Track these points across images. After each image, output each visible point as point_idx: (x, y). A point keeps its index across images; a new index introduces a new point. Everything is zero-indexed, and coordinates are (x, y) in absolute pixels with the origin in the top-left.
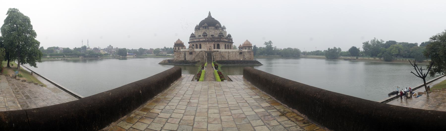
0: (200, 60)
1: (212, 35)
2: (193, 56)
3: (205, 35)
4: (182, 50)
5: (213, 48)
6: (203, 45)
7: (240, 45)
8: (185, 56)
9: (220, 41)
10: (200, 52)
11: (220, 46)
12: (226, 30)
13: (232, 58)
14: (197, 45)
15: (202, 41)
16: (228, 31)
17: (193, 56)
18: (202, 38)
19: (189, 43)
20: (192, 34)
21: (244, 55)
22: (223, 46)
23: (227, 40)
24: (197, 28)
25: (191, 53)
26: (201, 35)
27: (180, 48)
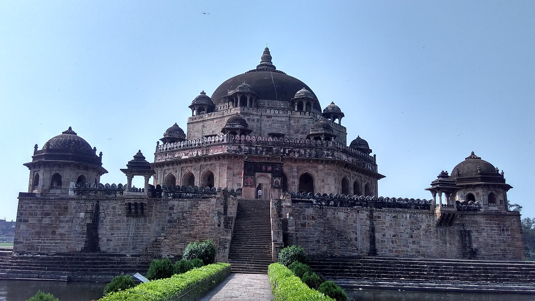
1: (273, 135)
7: (444, 175)
9: (318, 160)
11: (317, 184)
12: (344, 122)
14: (190, 178)
15: (218, 157)
18: (219, 144)
21: (465, 235)
26: (218, 131)
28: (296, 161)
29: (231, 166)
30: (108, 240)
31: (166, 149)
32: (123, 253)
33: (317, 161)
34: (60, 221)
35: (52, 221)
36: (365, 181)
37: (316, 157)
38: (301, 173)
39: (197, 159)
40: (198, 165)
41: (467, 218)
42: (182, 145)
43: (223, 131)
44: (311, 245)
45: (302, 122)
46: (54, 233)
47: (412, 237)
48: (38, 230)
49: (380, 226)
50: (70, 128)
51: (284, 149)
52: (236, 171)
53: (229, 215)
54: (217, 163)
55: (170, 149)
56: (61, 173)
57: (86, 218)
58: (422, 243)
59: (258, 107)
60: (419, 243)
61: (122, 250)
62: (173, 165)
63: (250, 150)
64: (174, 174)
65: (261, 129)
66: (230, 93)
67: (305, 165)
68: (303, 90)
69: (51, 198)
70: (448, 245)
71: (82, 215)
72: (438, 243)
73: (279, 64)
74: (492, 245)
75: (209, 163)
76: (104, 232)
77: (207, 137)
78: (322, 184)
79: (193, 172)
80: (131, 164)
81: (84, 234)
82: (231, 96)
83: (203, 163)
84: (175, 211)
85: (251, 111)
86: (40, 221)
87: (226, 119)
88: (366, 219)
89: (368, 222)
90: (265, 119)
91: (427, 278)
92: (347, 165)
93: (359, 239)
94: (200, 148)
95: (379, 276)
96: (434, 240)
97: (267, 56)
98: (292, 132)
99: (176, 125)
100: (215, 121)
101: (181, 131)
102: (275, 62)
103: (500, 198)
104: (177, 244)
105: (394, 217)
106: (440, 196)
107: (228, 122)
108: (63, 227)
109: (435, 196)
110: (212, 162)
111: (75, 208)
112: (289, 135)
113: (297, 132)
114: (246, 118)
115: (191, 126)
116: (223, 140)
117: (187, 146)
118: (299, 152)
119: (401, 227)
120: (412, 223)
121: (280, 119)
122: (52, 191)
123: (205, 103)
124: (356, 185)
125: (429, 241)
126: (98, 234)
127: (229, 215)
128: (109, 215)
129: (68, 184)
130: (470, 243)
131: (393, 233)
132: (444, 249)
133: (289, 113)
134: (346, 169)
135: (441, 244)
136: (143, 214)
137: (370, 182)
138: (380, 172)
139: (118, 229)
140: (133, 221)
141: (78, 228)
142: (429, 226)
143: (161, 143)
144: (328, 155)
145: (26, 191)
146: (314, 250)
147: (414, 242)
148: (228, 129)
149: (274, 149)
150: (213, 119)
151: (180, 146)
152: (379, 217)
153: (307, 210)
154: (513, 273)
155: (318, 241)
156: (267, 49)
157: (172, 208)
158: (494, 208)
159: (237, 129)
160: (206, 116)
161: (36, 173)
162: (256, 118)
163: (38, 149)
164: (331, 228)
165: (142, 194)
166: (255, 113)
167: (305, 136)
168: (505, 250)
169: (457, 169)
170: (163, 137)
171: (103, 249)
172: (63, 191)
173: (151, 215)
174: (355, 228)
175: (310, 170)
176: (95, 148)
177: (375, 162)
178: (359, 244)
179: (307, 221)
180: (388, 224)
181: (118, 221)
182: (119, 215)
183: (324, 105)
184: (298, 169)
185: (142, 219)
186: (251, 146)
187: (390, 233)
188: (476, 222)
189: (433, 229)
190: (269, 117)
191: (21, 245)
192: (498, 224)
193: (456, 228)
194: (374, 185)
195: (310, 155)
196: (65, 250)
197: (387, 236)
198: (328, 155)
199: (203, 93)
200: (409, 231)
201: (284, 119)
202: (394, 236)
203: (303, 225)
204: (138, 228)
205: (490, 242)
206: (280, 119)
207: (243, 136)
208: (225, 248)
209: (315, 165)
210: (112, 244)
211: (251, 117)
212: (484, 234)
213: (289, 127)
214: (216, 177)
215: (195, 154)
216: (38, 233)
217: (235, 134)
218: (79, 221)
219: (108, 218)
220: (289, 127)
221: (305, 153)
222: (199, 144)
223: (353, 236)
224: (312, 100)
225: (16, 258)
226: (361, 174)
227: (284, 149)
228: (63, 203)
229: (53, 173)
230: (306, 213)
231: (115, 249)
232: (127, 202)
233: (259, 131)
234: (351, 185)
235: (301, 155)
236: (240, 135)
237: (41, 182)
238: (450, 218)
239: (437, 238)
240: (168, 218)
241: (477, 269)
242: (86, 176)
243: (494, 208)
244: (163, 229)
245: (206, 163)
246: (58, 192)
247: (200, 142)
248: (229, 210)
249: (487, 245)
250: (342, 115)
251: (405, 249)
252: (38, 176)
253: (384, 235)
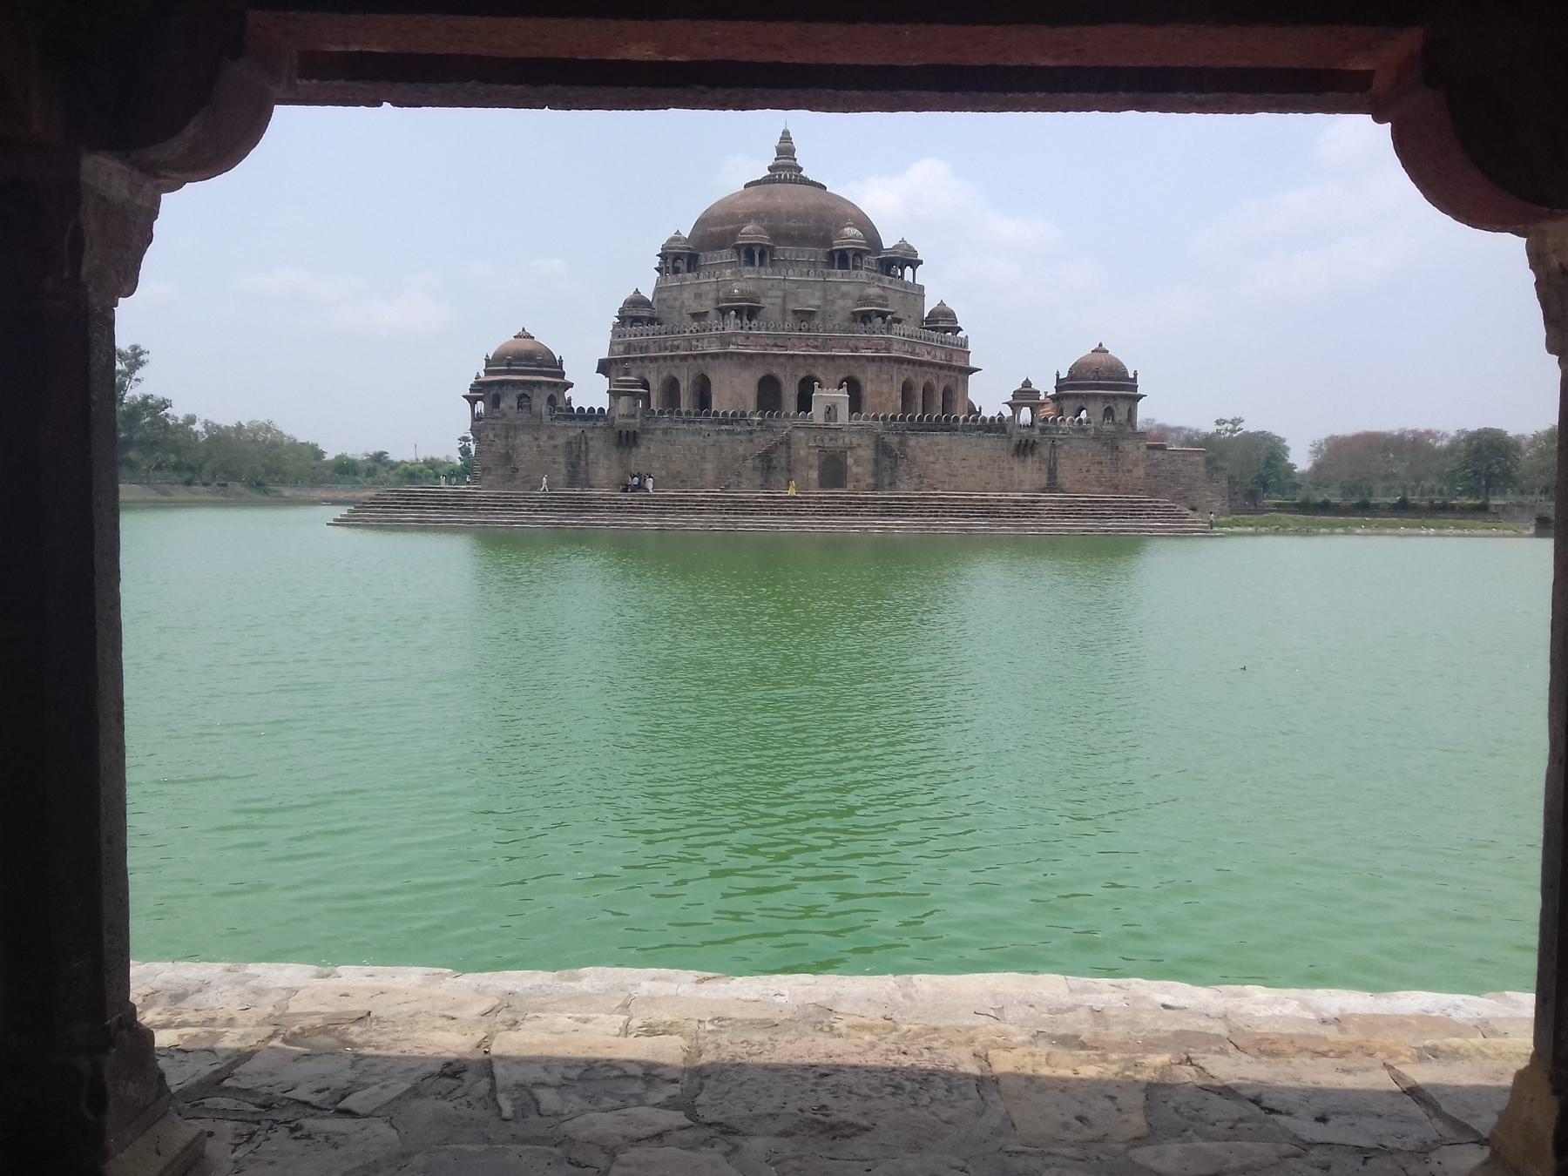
12: (923, 276)
14: (672, 386)
15: (715, 356)
16: (936, 285)
19: (604, 367)
20: (636, 302)
24: (678, 259)
26: (708, 305)
124: (928, 389)
138: (972, 364)
183: (888, 243)
194: (960, 387)
250: (915, 264)
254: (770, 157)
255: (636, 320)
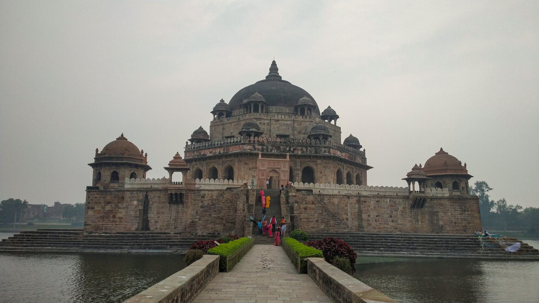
0: (219, 228)
2: (188, 213)
3: (250, 133)
4: (129, 184)
5: (285, 177)
6: (240, 170)
8: (145, 210)
10: (221, 193)
11: (317, 175)
12: (339, 123)
13: (377, 222)
15: (236, 155)
16: (347, 127)
17: (188, 213)
18: (236, 144)
21: (433, 214)
22: (332, 177)
23: (343, 155)
24: (221, 111)
25: (176, 197)
26: (236, 133)
27: (125, 173)
28: (299, 157)
29: (248, 162)
30: (156, 222)
31: (194, 148)
32: (166, 231)
33: (316, 157)
34: (119, 208)
35: (112, 208)
36: (356, 172)
37: (316, 152)
38: (303, 167)
39: (220, 156)
40: (220, 161)
41: (435, 202)
42: (207, 145)
43: (240, 133)
44: (312, 224)
45: (304, 125)
46: (114, 217)
47: (391, 217)
48: (102, 215)
49: (366, 208)
50: (122, 135)
51: (290, 148)
52: (251, 166)
53: (250, 203)
54: (236, 160)
55: (197, 148)
56: (118, 171)
57: (138, 205)
58: (399, 221)
59: (267, 112)
60: (397, 221)
61: (166, 229)
62: (200, 161)
63: (263, 150)
64: (201, 168)
65: (270, 131)
66: (245, 101)
67: (307, 160)
68: (305, 98)
69: (112, 190)
70: (420, 223)
71: (135, 203)
72: (411, 221)
73: (285, 74)
74: (455, 223)
75: (230, 159)
76: (153, 216)
77: (227, 137)
78: (321, 175)
79: (216, 167)
80: (171, 163)
81: (137, 217)
82: (244, 104)
83: (224, 159)
84: (206, 199)
85: (263, 117)
86: (104, 208)
87: (243, 123)
88: (355, 203)
89: (357, 206)
90: (273, 122)
91: (401, 248)
92: (340, 160)
93: (350, 219)
94: (222, 147)
95: (363, 247)
96: (409, 219)
97: (274, 67)
98: (296, 132)
99: (201, 128)
100: (233, 124)
101: (205, 133)
102: (281, 73)
103: (462, 185)
104: (208, 224)
105: (377, 201)
106: (414, 184)
107: (244, 125)
108: (121, 212)
109: (409, 184)
110: (232, 159)
111: (129, 197)
112: (293, 135)
113: (299, 133)
114: (258, 122)
115: (213, 128)
116: (240, 141)
117: (211, 145)
118: (302, 150)
119: (383, 209)
120: (392, 206)
121: (286, 122)
122: (112, 185)
123: (224, 109)
124: (349, 175)
125: (405, 220)
126: (147, 218)
127: (250, 203)
128: (155, 202)
129: (124, 179)
130: (437, 220)
131: (376, 214)
132: (416, 226)
133: (293, 117)
134: (340, 163)
135: (414, 222)
136: (182, 202)
137: (360, 172)
138: (368, 164)
139: (163, 213)
140: (174, 207)
141: (132, 213)
142: (404, 208)
143: (189, 143)
144: (325, 151)
145: (91, 185)
146: (314, 228)
147: (393, 221)
148: (244, 132)
149: (282, 147)
150: (231, 123)
151: (205, 146)
152: (365, 202)
153: (308, 197)
154: (468, 244)
155: (317, 221)
156: (274, 63)
157: (203, 197)
158: (456, 193)
159: (252, 132)
160: (225, 120)
161: (98, 171)
162: (266, 122)
163: (99, 152)
164: (327, 210)
165: (181, 186)
166: (265, 118)
167: (306, 136)
168: (465, 226)
169: (428, 163)
170: (191, 138)
171: (152, 228)
172: (120, 185)
173: (188, 202)
174: (347, 210)
175: (311, 164)
176: (142, 150)
177: (364, 156)
178: (350, 223)
179: (309, 206)
180: (372, 207)
181: (163, 207)
182: (164, 202)
184: (300, 163)
185: (181, 206)
186: (263, 145)
187: (373, 214)
188: (442, 205)
189: (408, 211)
190: (277, 121)
191: (89, 227)
192: (460, 206)
193: (426, 209)
195: (311, 152)
196: (123, 230)
197: (372, 216)
198: (325, 151)
199: (222, 101)
200: (389, 212)
201: (289, 123)
202: (377, 216)
203: (306, 209)
204: (178, 212)
205: (453, 220)
206: (286, 122)
207: (256, 137)
208: (250, 227)
209: (315, 160)
210: (158, 225)
211: (262, 121)
212: (449, 214)
213: (294, 128)
214: (236, 170)
215: (217, 151)
216: (102, 217)
217: (251, 136)
218: (133, 207)
219: (155, 205)
220: (294, 128)
221: (307, 151)
222: (221, 144)
223: (345, 216)
224: (312, 106)
225: (87, 236)
226: (352, 166)
227: (290, 148)
228: (120, 194)
229: (112, 171)
230: (307, 200)
231: (161, 229)
232: (169, 192)
233: (269, 133)
234: (345, 176)
235: (303, 152)
236: (254, 137)
237: (103, 178)
238: (421, 202)
239: (411, 217)
240: (200, 204)
241: (440, 241)
242: (136, 173)
243: (456, 193)
244: (197, 213)
245: (226, 160)
246: (116, 185)
247: (222, 143)
248: (250, 199)
249: (452, 222)
250: (337, 117)
251: (386, 226)
252: (99, 174)
253: (369, 216)
254: (267, 72)
255: (199, 141)
